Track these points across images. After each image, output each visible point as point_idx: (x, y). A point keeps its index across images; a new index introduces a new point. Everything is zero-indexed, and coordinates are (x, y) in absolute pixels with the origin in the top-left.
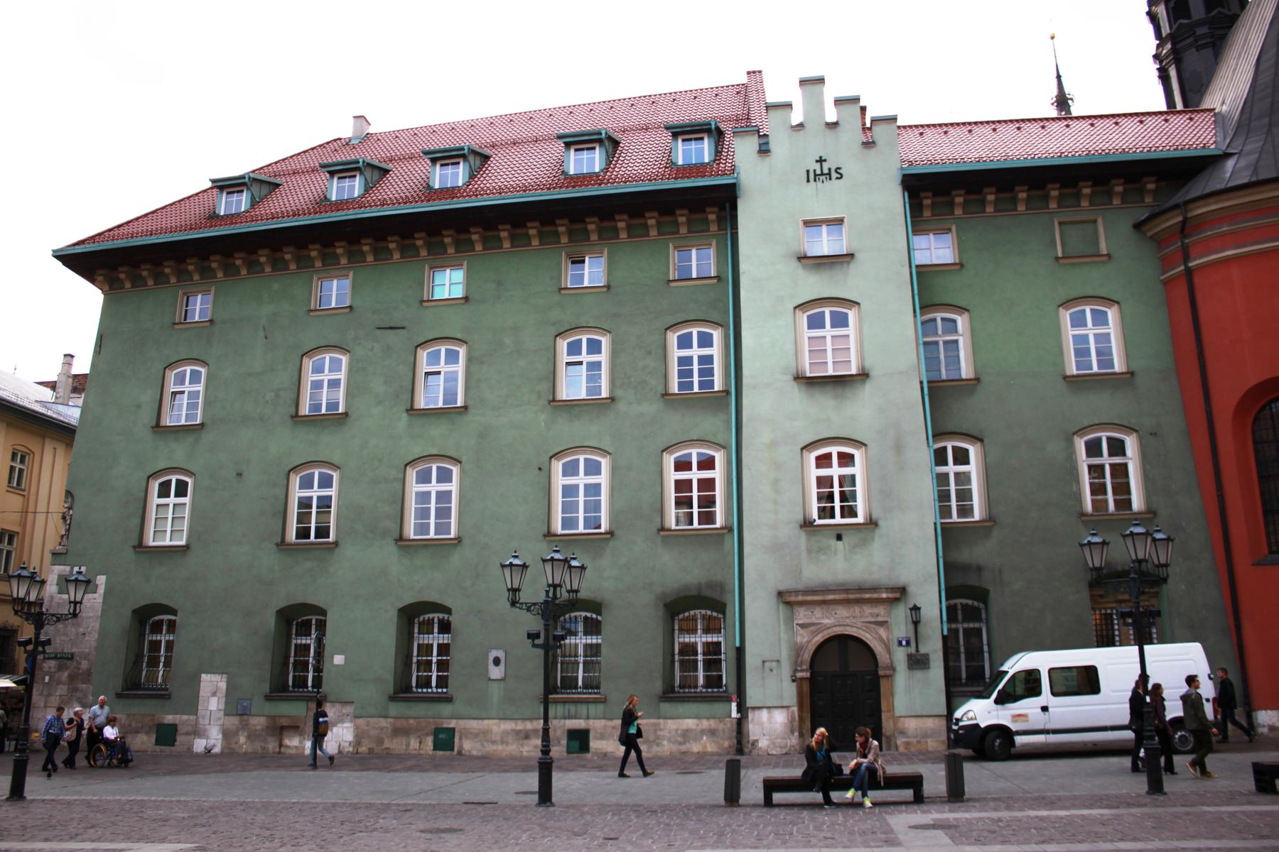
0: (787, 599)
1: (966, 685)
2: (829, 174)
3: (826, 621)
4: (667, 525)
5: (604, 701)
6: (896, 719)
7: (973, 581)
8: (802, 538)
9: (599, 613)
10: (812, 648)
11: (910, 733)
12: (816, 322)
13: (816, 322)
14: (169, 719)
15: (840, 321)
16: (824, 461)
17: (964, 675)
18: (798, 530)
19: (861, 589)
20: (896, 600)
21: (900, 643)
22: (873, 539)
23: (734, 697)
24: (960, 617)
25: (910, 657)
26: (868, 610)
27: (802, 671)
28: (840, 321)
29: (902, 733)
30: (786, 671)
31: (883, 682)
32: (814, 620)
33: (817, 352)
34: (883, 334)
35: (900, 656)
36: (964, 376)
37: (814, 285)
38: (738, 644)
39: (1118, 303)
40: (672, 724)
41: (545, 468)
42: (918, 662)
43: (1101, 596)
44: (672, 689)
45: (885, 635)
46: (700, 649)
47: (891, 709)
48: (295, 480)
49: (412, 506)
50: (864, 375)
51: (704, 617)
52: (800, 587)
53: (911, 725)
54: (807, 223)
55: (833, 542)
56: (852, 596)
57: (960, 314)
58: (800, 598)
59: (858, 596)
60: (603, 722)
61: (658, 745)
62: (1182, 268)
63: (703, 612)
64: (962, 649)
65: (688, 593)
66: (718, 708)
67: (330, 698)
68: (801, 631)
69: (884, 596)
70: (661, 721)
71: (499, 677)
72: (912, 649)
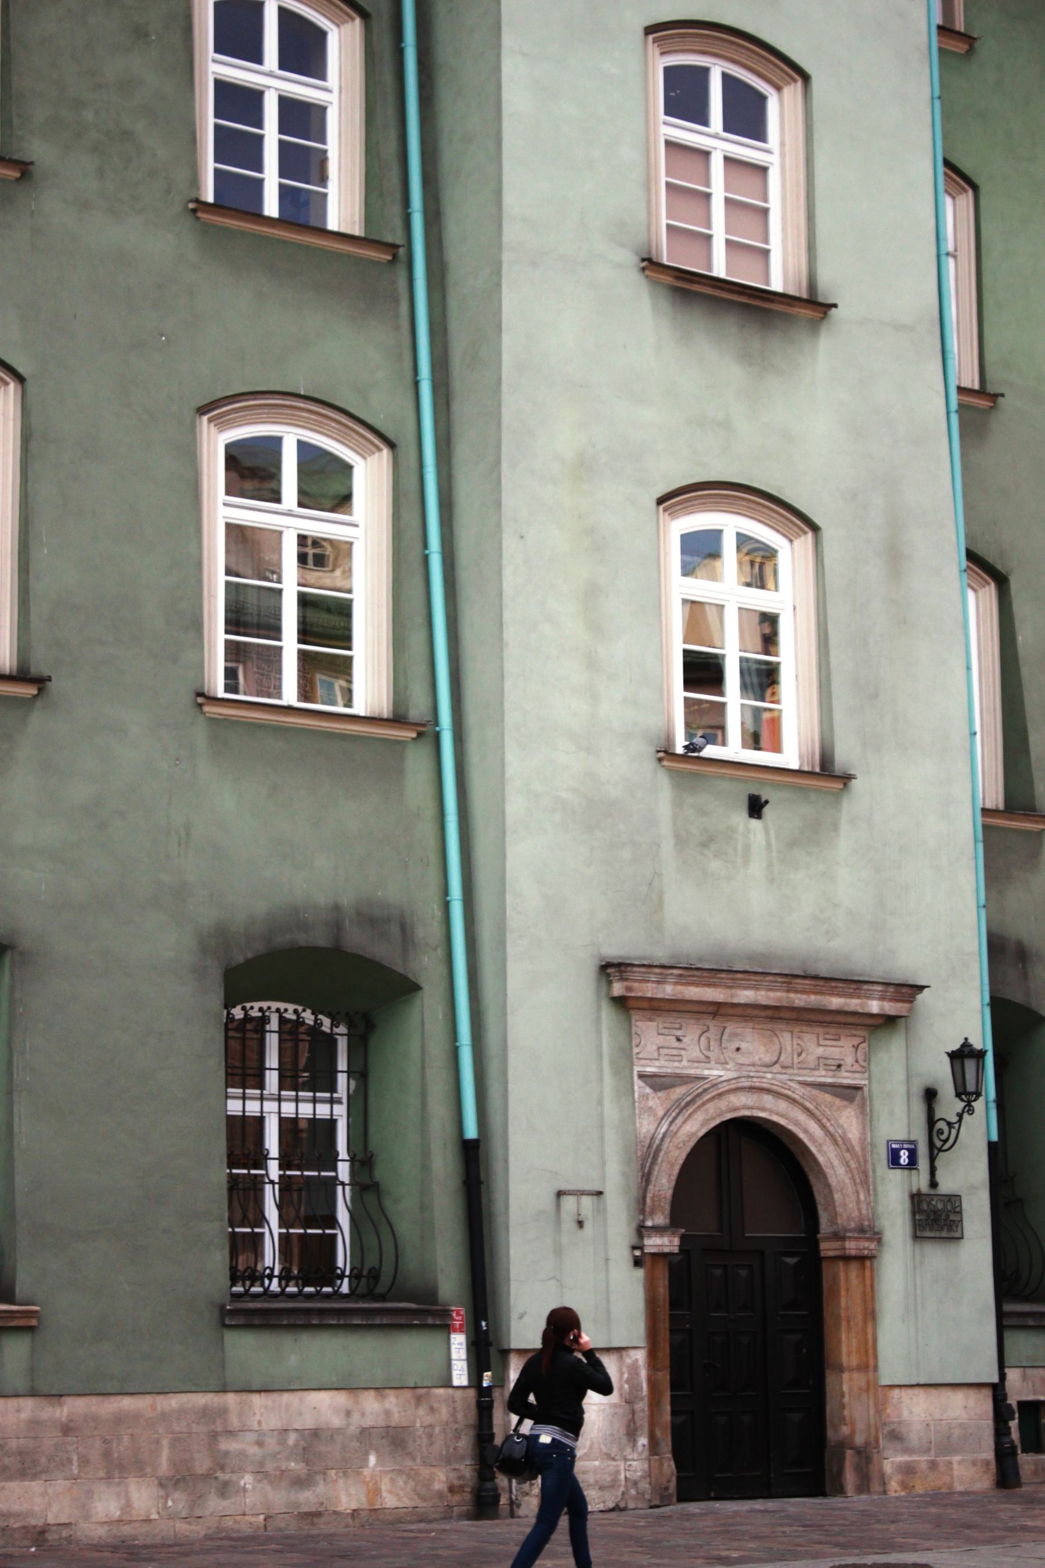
0: (626, 989)
3: (714, 1072)
6: (878, 1393)
8: (661, 793)
10: (675, 1155)
11: (915, 1435)
13: (685, 96)
15: (746, 116)
18: (650, 764)
20: (889, 1022)
21: (894, 1159)
22: (835, 827)
23: (459, 1314)
25: (916, 1199)
27: (658, 1230)
31: (849, 1278)
35: (893, 1196)
40: (264, 1412)
45: (862, 1123)
46: (272, 1143)
47: (869, 1363)
50: (811, 307)
51: (290, 1030)
52: (660, 954)
53: (916, 1410)
55: (740, 817)
58: (669, 990)
60: (28, 1407)
61: (224, 1490)
63: (290, 1009)
65: (302, 939)
66: (409, 1349)
70: (231, 1398)
72: (921, 1180)
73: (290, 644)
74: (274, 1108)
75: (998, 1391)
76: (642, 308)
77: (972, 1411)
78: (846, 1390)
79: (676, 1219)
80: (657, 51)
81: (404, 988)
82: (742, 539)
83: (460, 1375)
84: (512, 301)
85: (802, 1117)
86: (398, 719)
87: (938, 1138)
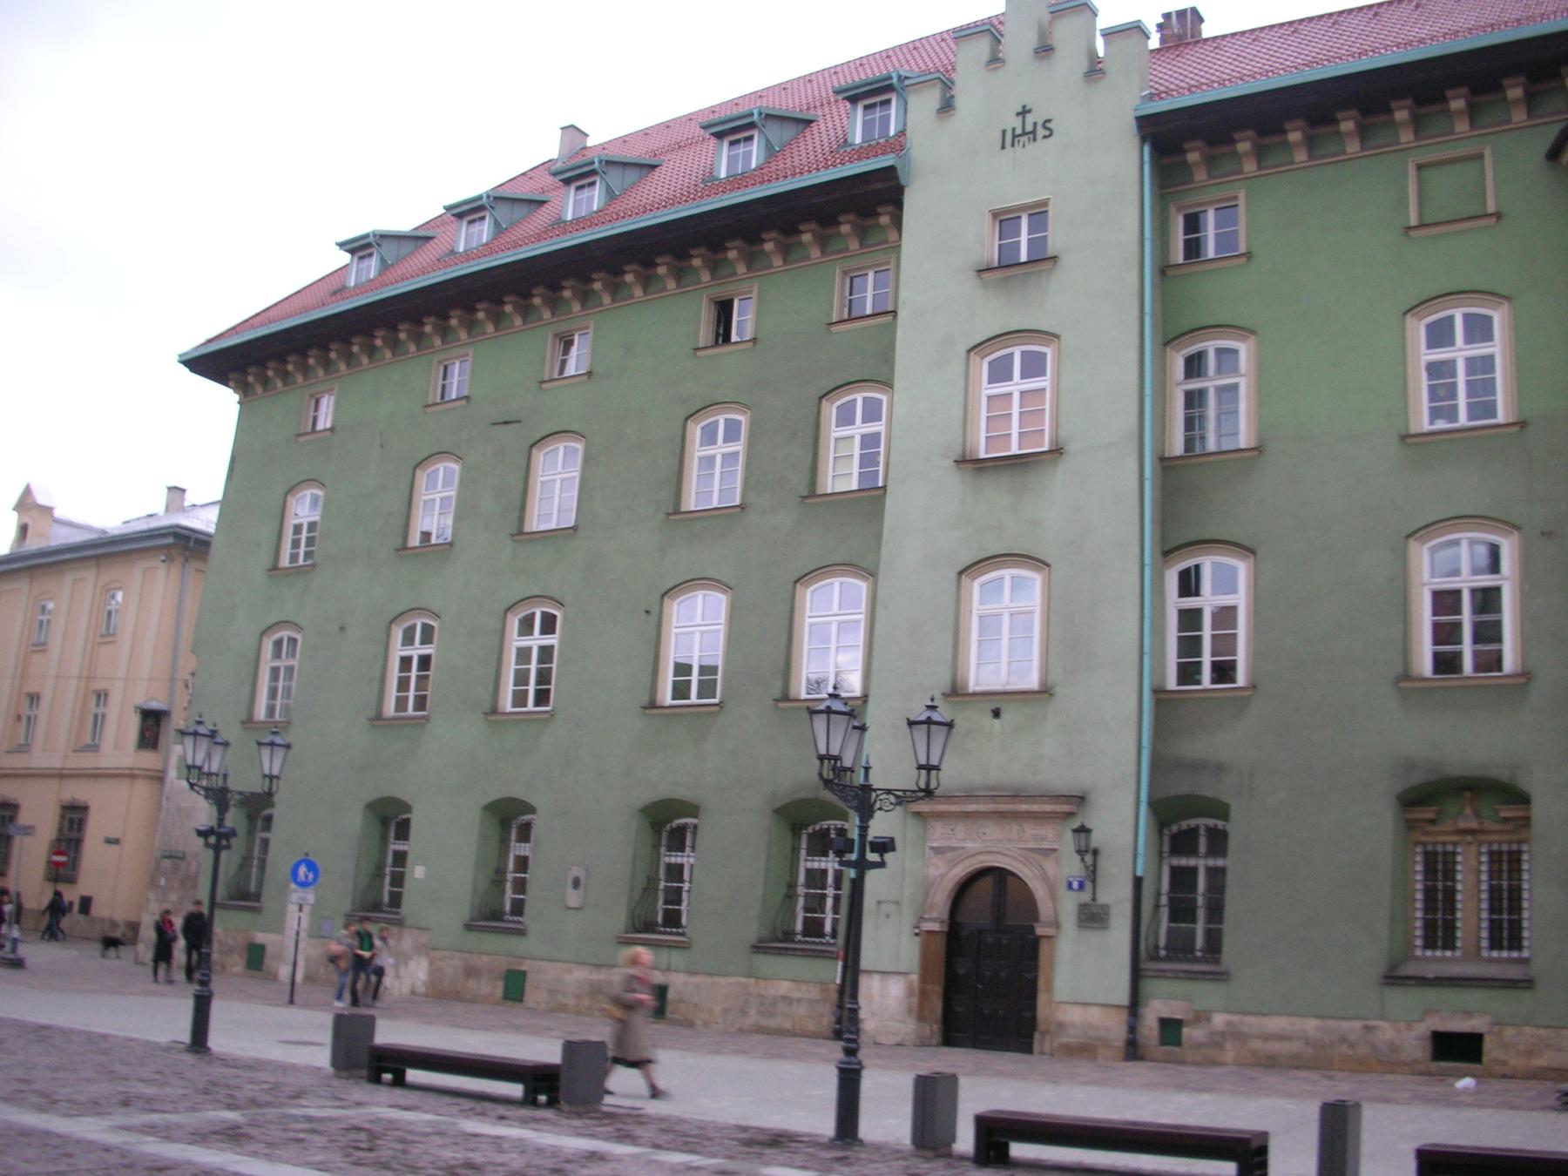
1: (1168, 959)
2: (1034, 132)
3: (970, 845)
4: (792, 695)
7: (1207, 788)
9: (696, 816)
12: (1000, 372)
14: (260, 938)
17: (1200, 941)
19: (1017, 795)
21: (1070, 886)
24: (1202, 848)
25: (1083, 907)
26: (1031, 830)
28: (1034, 366)
30: (907, 918)
31: (1044, 947)
32: (954, 843)
33: (998, 419)
34: (1092, 379)
35: (1069, 904)
36: (1242, 446)
37: (994, 314)
39: (1507, 298)
41: (655, 610)
42: (1093, 917)
43: (1432, 821)
44: (788, 935)
45: (1045, 869)
47: (1049, 990)
48: (398, 635)
49: (511, 666)
50: (1057, 451)
53: (1074, 1015)
55: (988, 720)
56: (1002, 807)
57: (1243, 339)
59: (1010, 807)
64: (1200, 901)
65: (802, 795)
67: (408, 922)
68: (936, 860)
69: (1048, 808)
70: (752, 980)
72: (1085, 897)
78: (1042, 999)
80: (978, 359)
83: (838, 981)
85: (1020, 866)
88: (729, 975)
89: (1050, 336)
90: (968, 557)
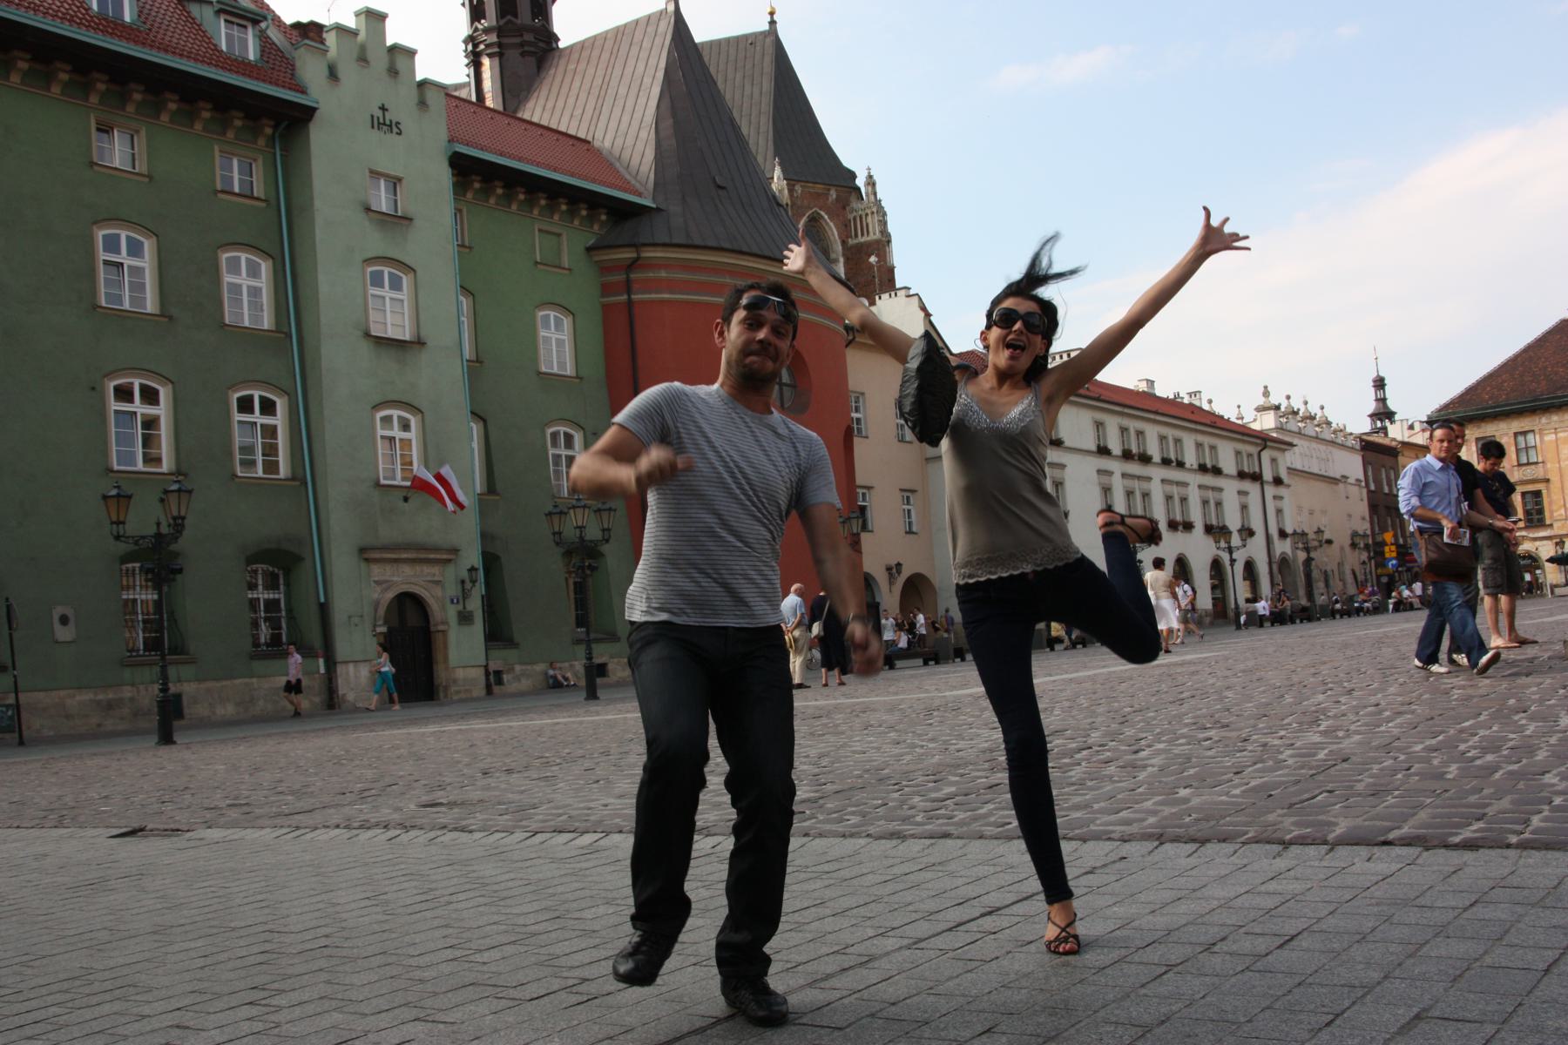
5: (193, 662)
12: (377, 280)
16: (387, 420)
23: (320, 652)
26: (427, 569)
29: (455, 681)
35: (452, 612)
38: (322, 600)
42: (465, 618)
45: (439, 590)
50: (419, 342)
54: (372, 172)
55: (401, 504)
62: (625, 297)
71: (69, 639)
72: (460, 607)
73: (260, 459)
74: (262, 595)
75: (486, 667)
76: (365, 347)
77: (479, 673)
79: (386, 622)
81: (298, 559)
82: (399, 417)
83: (322, 671)
84: (324, 351)
86: (293, 479)
87: (465, 595)
88: (232, 677)
89: (409, 269)
90: (378, 399)
